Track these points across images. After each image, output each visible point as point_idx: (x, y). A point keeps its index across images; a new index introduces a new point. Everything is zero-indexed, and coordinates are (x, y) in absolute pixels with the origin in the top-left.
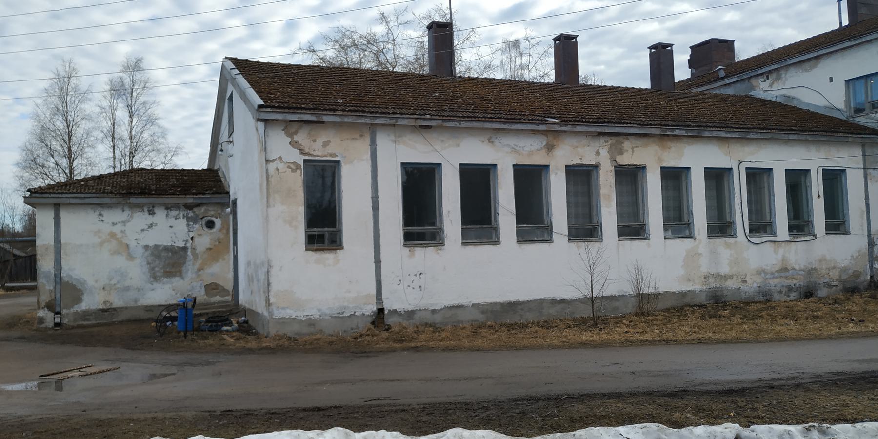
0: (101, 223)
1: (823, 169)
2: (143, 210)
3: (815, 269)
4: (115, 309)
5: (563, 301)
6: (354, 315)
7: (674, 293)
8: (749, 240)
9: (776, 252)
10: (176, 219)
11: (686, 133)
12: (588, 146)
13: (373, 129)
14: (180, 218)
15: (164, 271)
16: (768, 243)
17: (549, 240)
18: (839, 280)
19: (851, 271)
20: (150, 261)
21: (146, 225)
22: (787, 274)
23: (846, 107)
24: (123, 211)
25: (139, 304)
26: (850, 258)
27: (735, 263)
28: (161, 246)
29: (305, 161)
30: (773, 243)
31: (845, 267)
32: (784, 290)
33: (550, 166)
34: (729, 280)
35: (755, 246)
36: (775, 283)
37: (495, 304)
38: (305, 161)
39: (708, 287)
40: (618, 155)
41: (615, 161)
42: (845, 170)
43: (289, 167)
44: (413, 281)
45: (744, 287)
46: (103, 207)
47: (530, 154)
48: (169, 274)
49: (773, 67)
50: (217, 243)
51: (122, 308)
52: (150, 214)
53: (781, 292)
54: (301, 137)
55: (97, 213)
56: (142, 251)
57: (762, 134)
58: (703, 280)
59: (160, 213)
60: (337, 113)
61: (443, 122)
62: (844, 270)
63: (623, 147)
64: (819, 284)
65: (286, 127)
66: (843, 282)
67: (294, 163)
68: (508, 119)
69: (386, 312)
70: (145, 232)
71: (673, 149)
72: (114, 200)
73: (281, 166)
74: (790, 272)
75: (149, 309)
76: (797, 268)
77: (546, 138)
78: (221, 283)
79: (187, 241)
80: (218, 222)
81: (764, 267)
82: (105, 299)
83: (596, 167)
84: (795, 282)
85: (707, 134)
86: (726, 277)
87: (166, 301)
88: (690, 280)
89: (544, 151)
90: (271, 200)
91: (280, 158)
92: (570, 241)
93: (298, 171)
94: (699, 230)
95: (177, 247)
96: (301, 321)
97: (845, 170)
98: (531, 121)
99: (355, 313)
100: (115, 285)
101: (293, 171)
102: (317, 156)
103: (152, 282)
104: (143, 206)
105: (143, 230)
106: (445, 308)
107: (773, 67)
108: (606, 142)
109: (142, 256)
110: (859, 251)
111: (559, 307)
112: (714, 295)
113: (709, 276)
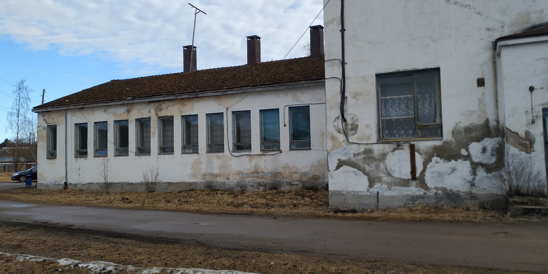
1: (289, 107)
3: (280, 173)
5: (132, 184)
6: (59, 184)
7: (186, 183)
8: (232, 155)
9: (250, 161)
11: (189, 96)
12: (145, 108)
13: (66, 111)
17: (127, 155)
18: (300, 181)
19: (310, 176)
22: (258, 175)
26: (310, 166)
27: (223, 168)
30: (248, 156)
31: (306, 172)
32: (255, 185)
34: (218, 177)
35: (236, 158)
36: (249, 180)
39: (205, 181)
40: (159, 112)
41: (158, 114)
43: (43, 129)
45: (227, 182)
47: (121, 115)
53: (253, 186)
57: (236, 91)
58: (203, 176)
60: (55, 107)
62: (305, 174)
63: (162, 107)
64: (283, 183)
65: (43, 113)
66: (303, 183)
68: (111, 100)
69: (68, 184)
71: (188, 105)
74: (261, 174)
76: (266, 171)
77: (127, 107)
81: (242, 170)
83: (149, 119)
84: (264, 180)
85: (201, 95)
86: (216, 176)
88: (195, 176)
89: (126, 113)
92: (136, 156)
94: (201, 149)
96: (45, 185)
97: (309, 106)
98: (120, 100)
101: (44, 130)
106: (87, 183)
108: (154, 106)
110: (319, 162)
112: (209, 185)
113: (206, 175)
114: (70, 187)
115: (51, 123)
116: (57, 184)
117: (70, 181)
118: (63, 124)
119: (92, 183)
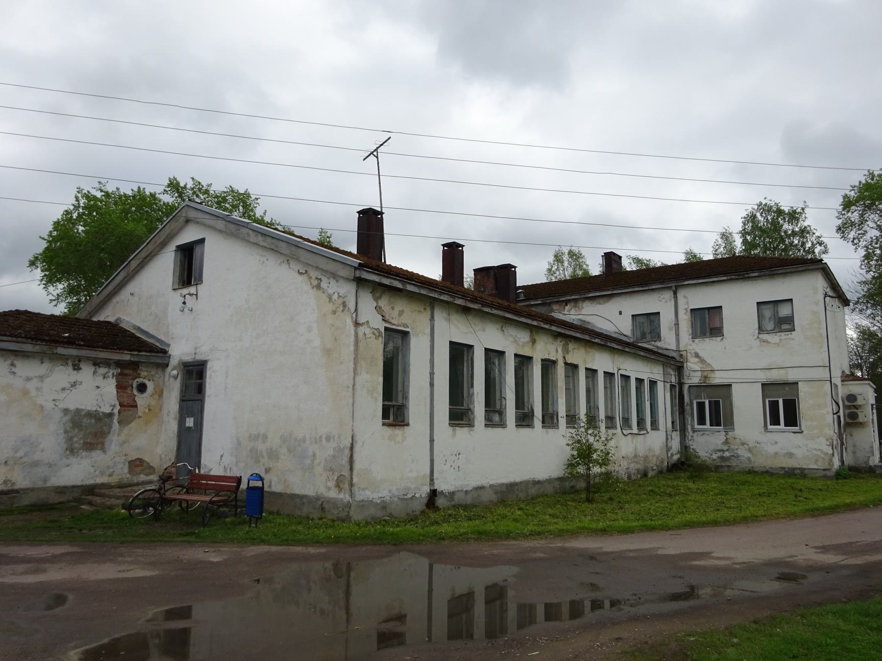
0: (12, 376)
2: (67, 364)
3: (647, 456)
4: (17, 491)
6: (414, 496)
8: (622, 432)
10: (104, 378)
11: (601, 341)
14: (108, 377)
15: (84, 442)
16: (629, 435)
20: (68, 429)
21: (69, 382)
23: (632, 334)
24: (42, 363)
25: (49, 484)
28: (84, 410)
29: (386, 329)
33: (534, 359)
37: (503, 484)
38: (386, 329)
42: (657, 382)
43: (373, 333)
44: (454, 461)
46: (17, 356)
48: (90, 447)
49: (573, 297)
50: (147, 410)
51: (27, 489)
52: (74, 369)
54: (384, 303)
55: (9, 362)
56: (60, 414)
59: (87, 371)
61: (482, 306)
67: (378, 329)
70: (68, 391)
71: (590, 354)
72: (37, 348)
73: (368, 331)
74: (638, 458)
75: (61, 490)
76: (641, 456)
78: (146, 458)
79: (114, 406)
80: (150, 385)
82: (6, 477)
87: (82, 481)
90: (359, 368)
91: (368, 322)
93: (380, 338)
95: (103, 413)
99: (415, 494)
100: (21, 458)
101: (377, 338)
102: (394, 325)
103: (67, 455)
104: (67, 359)
105: (63, 389)
107: (573, 297)
109: (60, 422)
110: (663, 443)
111: (538, 486)
114: (440, 502)
115: (397, 323)
116: (409, 496)
117: (442, 486)
118: (425, 334)
119: (481, 488)
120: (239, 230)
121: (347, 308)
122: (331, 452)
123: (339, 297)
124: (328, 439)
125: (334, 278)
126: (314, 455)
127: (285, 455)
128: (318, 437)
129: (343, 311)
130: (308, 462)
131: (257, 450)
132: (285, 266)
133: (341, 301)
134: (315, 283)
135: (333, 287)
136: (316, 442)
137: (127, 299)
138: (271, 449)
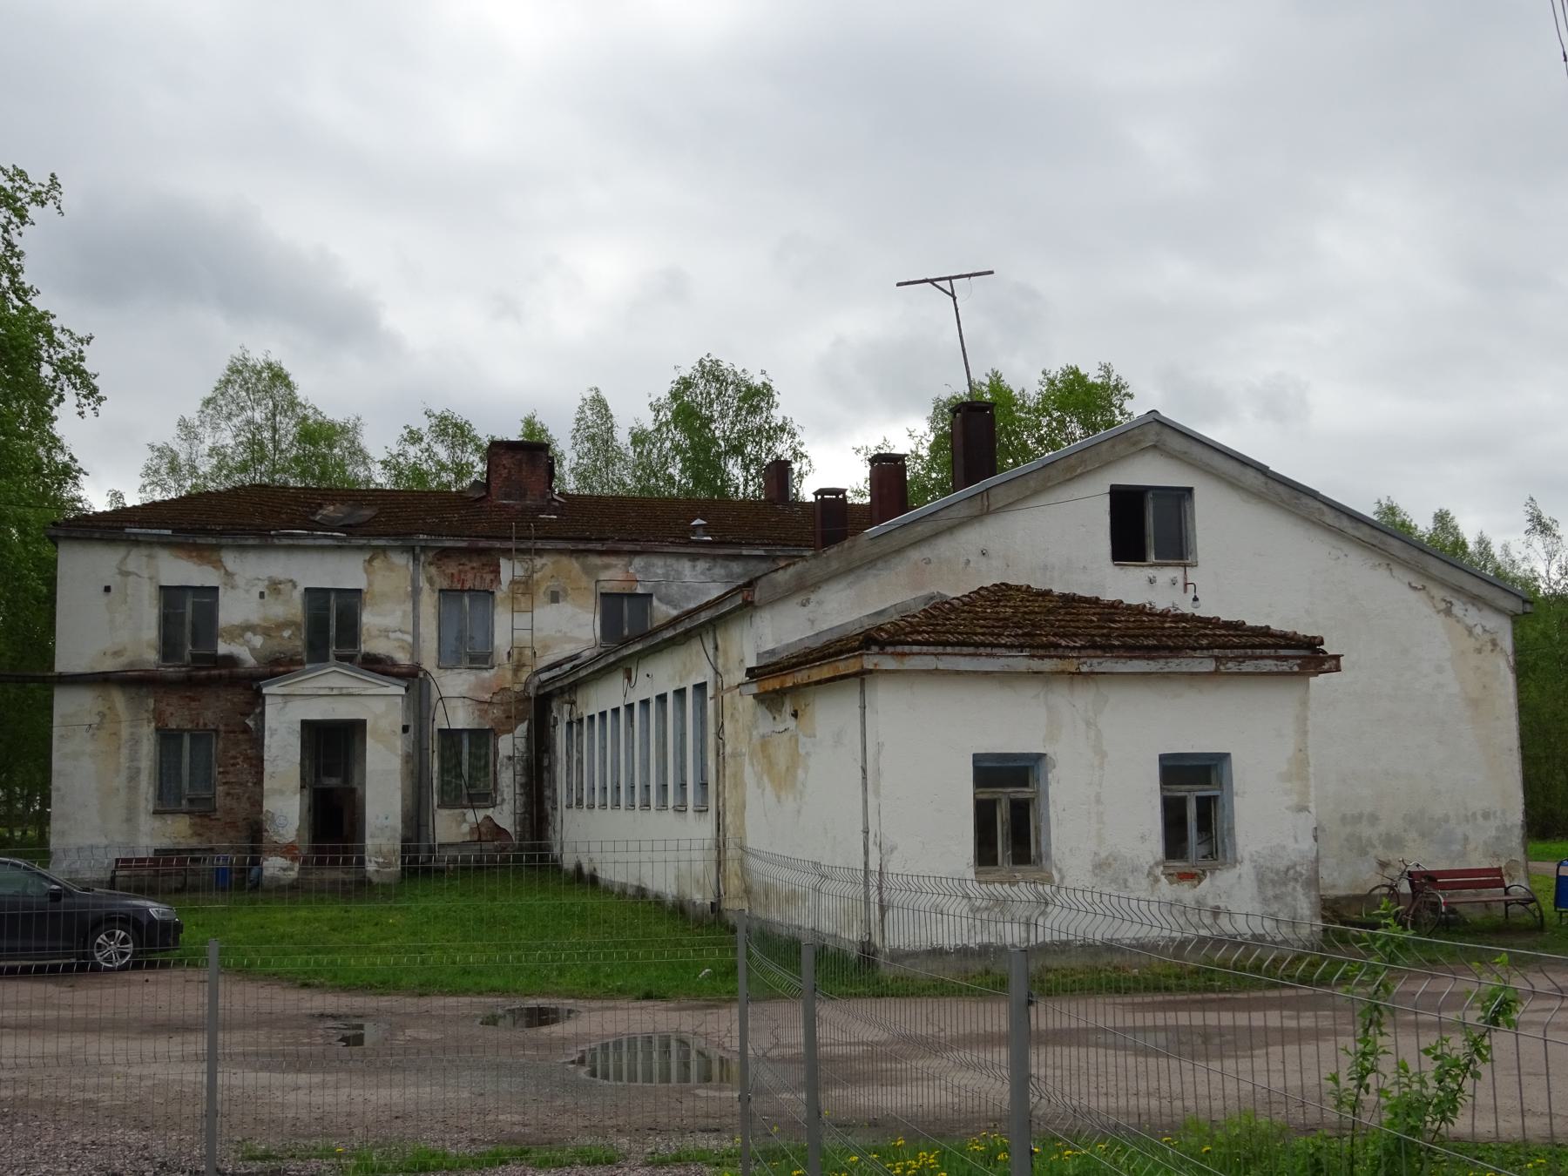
120: (1298, 499)
121: (1498, 649)
122: (1494, 833)
123: (1485, 631)
124: (1486, 816)
125: (1473, 605)
126: (1466, 839)
127: (1414, 841)
128: (1470, 814)
129: (1492, 651)
130: (1456, 847)
131: (1360, 838)
132: (1382, 573)
133: (1487, 637)
134: (1443, 606)
135: (1473, 616)
136: (1468, 821)
137: (963, 560)
138: (1387, 834)
